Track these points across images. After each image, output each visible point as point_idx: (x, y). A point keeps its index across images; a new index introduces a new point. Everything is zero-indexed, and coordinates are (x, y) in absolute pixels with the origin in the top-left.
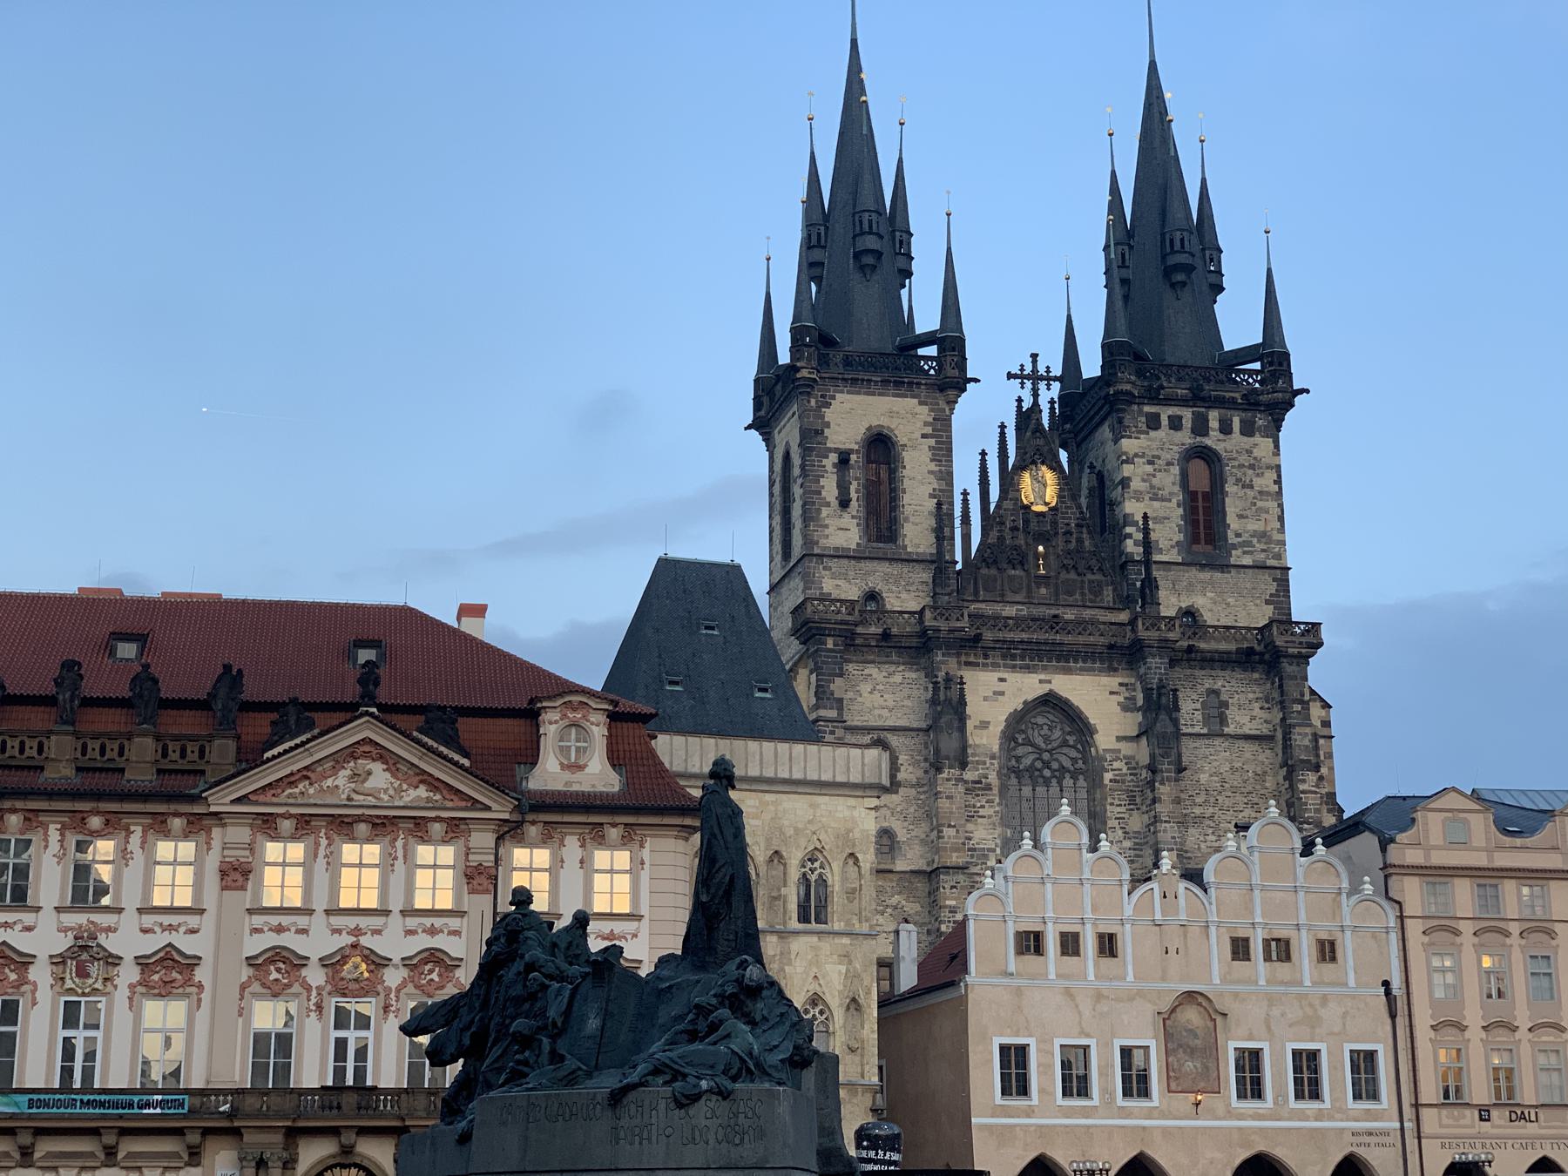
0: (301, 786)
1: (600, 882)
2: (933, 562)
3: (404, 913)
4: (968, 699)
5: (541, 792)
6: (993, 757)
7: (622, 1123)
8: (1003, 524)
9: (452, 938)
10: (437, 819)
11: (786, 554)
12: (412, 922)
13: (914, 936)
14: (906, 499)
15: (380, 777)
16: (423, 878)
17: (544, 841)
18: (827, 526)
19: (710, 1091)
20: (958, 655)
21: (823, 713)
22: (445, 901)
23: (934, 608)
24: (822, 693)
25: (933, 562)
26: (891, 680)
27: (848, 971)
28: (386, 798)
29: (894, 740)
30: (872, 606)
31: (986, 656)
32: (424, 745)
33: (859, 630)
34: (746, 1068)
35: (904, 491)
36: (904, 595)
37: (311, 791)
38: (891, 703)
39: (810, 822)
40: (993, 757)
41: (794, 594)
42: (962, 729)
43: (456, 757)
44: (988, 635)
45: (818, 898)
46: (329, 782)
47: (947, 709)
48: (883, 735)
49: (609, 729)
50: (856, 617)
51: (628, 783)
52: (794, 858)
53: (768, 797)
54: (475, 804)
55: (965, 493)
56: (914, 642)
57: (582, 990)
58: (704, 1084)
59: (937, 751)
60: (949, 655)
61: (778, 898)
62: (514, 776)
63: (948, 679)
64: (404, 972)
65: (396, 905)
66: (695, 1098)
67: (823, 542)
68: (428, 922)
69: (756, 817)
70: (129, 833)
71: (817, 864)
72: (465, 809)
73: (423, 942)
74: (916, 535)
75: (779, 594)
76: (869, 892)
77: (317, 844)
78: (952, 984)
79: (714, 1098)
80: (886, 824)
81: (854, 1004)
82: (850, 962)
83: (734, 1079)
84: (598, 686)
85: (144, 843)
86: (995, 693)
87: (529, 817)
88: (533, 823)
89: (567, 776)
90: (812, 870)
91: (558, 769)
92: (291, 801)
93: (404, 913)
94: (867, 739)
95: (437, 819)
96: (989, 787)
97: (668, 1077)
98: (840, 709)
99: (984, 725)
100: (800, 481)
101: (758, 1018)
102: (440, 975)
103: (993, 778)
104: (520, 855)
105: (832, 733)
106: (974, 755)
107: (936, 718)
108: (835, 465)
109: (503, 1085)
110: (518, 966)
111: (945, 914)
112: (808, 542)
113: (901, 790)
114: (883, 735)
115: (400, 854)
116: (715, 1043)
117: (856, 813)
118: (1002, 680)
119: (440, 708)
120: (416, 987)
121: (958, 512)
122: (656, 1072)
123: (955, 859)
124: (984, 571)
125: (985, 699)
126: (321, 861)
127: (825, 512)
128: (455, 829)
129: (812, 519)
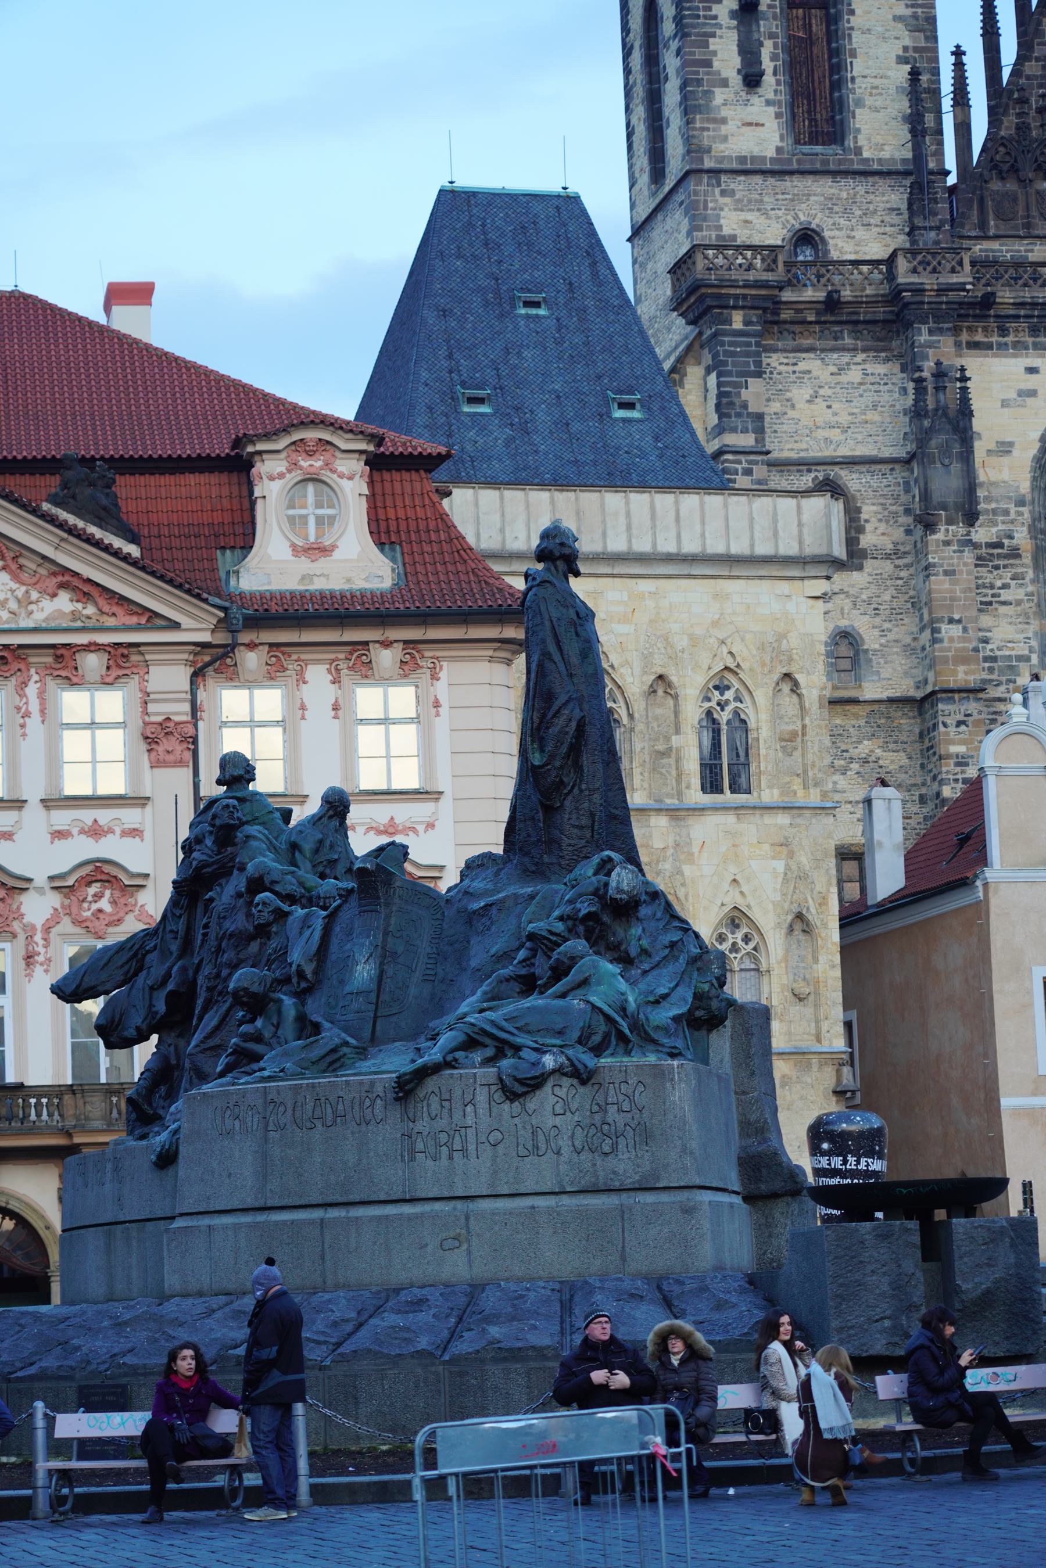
1: (368, 739)
2: (906, 173)
3: (47, 803)
4: (976, 405)
5: (262, 597)
6: (1021, 502)
7: (419, 1126)
8: (1023, 101)
9: (128, 840)
10: (93, 647)
11: (658, 174)
12: (62, 818)
13: (897, 806)
14: (858, 67)
16: (74, 745)
17: (273, 674)
18: (724, 121)
19: (558, 1071)
20: (956, 331)
21: (731, 439)
22: (114, 783)
23: (912, 252)
24: (726, 406)
25: (906, 173)
26: (843, 378)
27: (788, 867)
29: (853, 480)
30: (806, 254)
31: (1003, 332)
32: (62, 525)
33: (787, 295)
34: (619, 1032)
35: (853, 54)
36: (860, 233)
38: (844, 419)
39: (715, 624)
40: (1021, 502)
41: (673, 240)
42: (967, 456)
43: (117, 543)
44: (1006, 296)
45: (733, 749)
47: (942, 422)
48: (834, 472)
49: (371, 483)
50: (780, 274)
51: (408, 572)
52: (691, 686)
53: (645, 585)
54: (153, 619)
55: (958, 53)
56: (881, 312)
57: (344, 916)
58: (549, 1061)
59: (926, 496)
60: (941, 331)
61: (666, 754)
62: (214, 570)
63: (940, 374)
64: (54, 900)
65: (33, 791)
66: (535, 1083)
67: (719, 148)
68: (87, 816)
69: (625, 619)
71: (729, 695)
72: (138, 628)
73: (85, 849)
74: (877, 128)
75: (648, 240)
76: (818, 739)
78: (964, 883)
79: (566, 1082)
80: (843, 623)
81: (800, 923)
82: (791, 855)
83: (598, 1051)
84: (347, 410)
86: (1021, 393)
87: (245, 638)
88: (252, 646)
89: (304, 565)
90: (722, 705)
91: (287, 553)
93: (47, 803)
94: (807, 480)
95: (93, 647)
96: (1015, 553)
97: (490, 1052)
98: (760, 431)
99: (1005, 448)
100: (674, 45)
101: (633, 952)
102: (114, 902)
103: (1022, 537)
104: (231, 701)
105: (748, 472)
106: (988, 499)
107: (922, 439)
108: (733, 15)
109: (222, 1075)
110: (237, 883)
111: (948, 768)
112: (693, 149)
113: (869, 565)
114: (834, 472)
115: (34, 706)
116: (563, 996)
117: (791, 607)
118: (1032, 370)
119: (88, 462)
120: (77, 922)
121: (947, 85)
122: (470, 1043)
123: (963, 675)
124: (996, 185)
125: (1005, 404)
127: (719, 96)
128: (122, 661)
129: (698, 109)
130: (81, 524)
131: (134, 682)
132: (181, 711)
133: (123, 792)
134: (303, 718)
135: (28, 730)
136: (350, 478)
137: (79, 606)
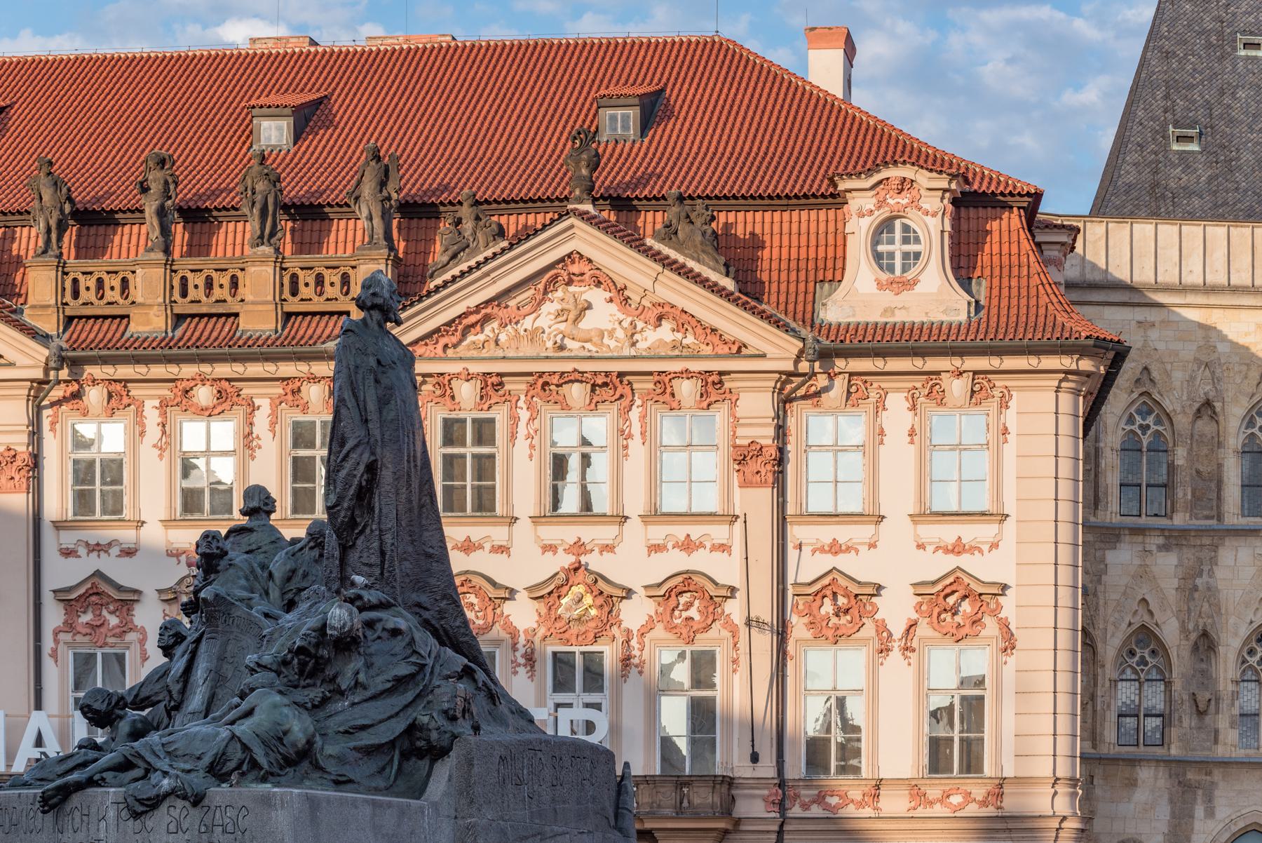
0: (488, 329)
1: (943, 463)
10: (688, 375)
12: (658, 533)
15: (603, 313)
22: (709, 501)
28: (613, 344)
37: (503, 337)
46: (527, 323)
49: (956, 220)
68: (680, 531)
70: (254, 408)
77: (515, 420)
85: (273, 424)
89: (888, 298)
91: (872, 287)
92: (474, 353)
95: (688, 375)
115: (636, 429)
126: (522, 445)
128: (714, 386)
130: (681, 259)
131: (725, 407)
132: (765, 435)
133: (713, 510)
134: (881, 443)
135: (630, 451)
136: (934, 215)
137: (679, 336)
